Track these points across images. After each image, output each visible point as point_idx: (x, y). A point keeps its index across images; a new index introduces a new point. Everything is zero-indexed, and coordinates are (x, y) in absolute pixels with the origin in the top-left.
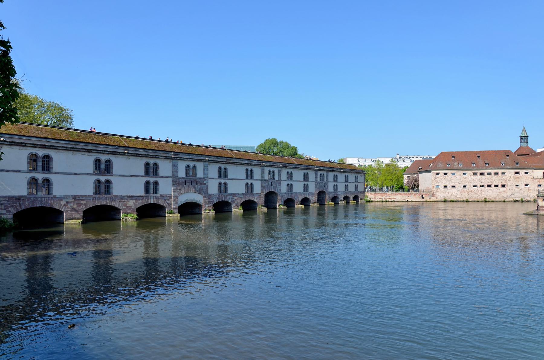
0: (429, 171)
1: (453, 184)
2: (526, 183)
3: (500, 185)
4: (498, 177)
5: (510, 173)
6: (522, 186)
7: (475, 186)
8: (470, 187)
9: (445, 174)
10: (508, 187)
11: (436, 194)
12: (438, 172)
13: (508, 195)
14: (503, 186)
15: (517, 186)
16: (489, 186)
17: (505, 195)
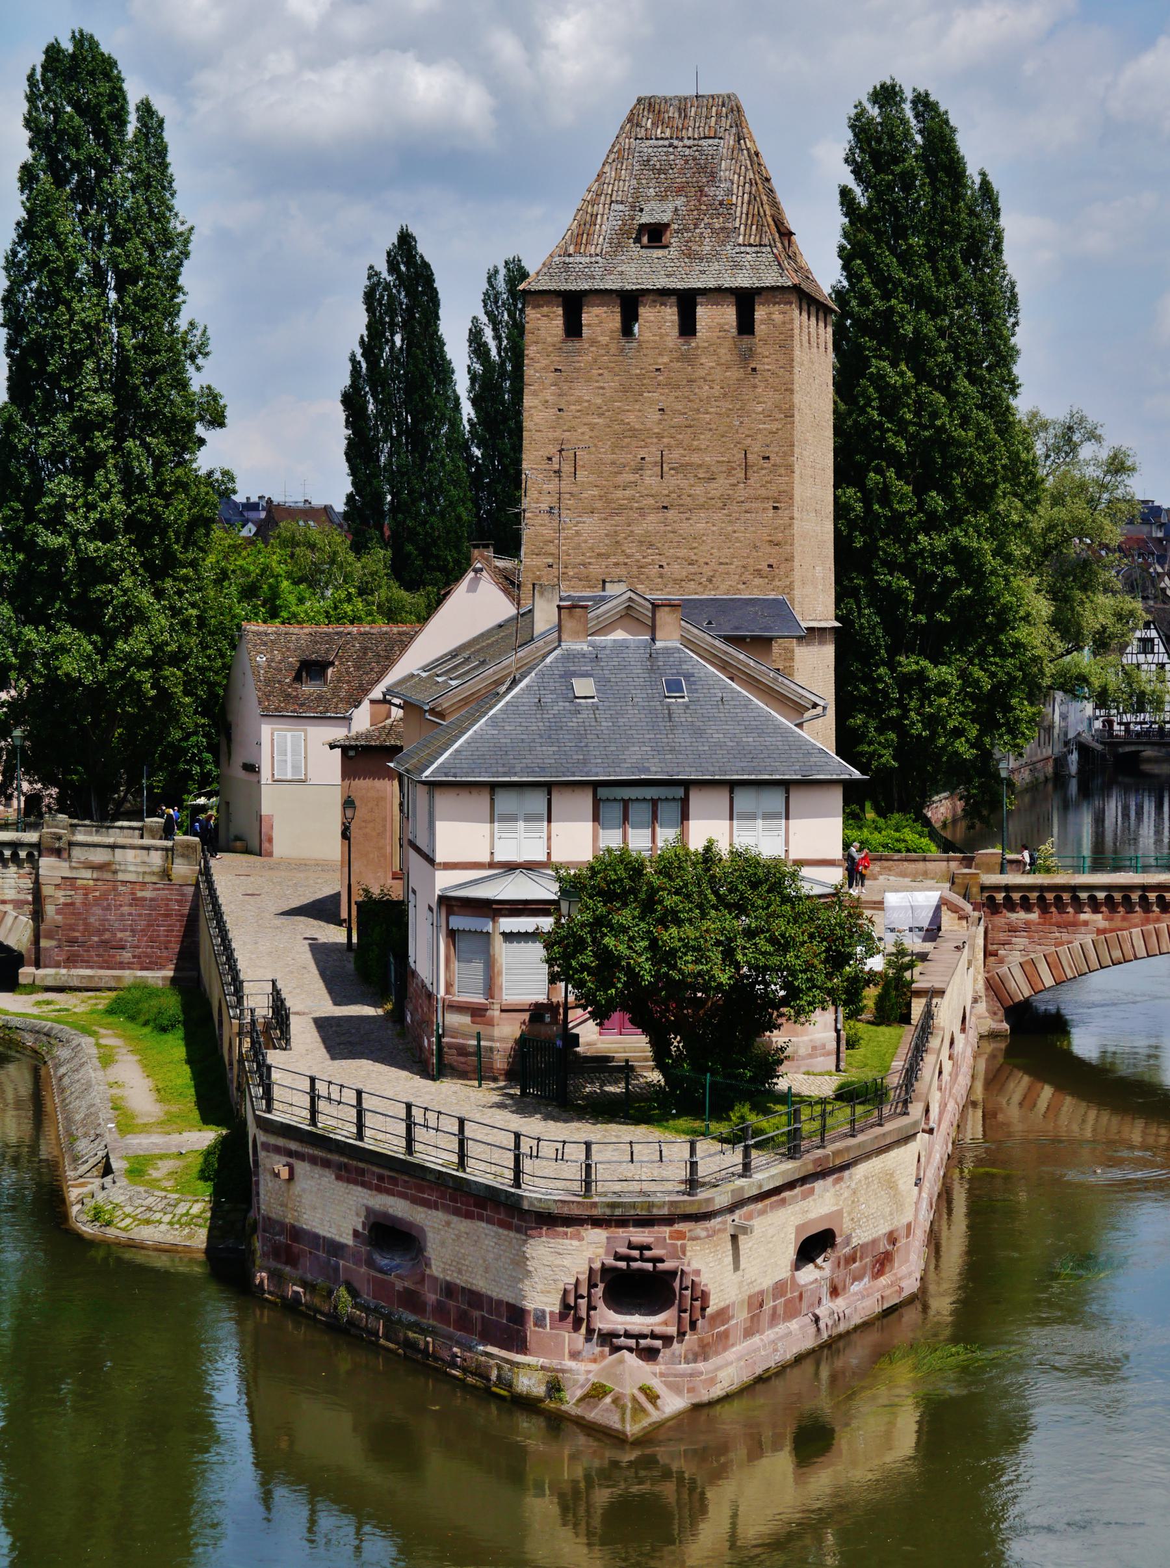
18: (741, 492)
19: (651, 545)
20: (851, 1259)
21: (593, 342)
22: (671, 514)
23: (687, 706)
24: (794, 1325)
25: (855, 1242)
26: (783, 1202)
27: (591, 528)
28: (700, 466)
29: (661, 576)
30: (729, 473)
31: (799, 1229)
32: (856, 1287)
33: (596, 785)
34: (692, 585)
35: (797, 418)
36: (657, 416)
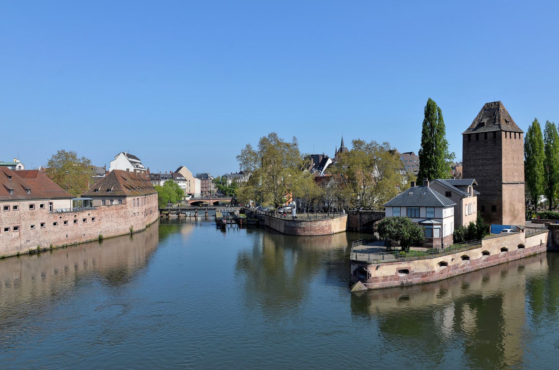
2: (42, 222)
3: (12, 228)
4: (9, 214)
5: (24, 205)
10: (22, 230)
13: (23, 243)
14: (16, 228)
15: (32, 227)
17: (17, 244)
18: (494, 162)
19: (481, 171)
20: (413, 275)
21: (472, 141)
22: (484, 166)
23: (424, 196)
24: (396, 282)
25: (415, 272)
26: (392, 264)
27: (472, 169)
28: (488, 159)
29: (482, 176)
30: (492, 160)
31: (397, 268)
32: (416, 278)
33: (407, 207)
34: (487, 177)
35: (503, 150)
36: (481, 152)
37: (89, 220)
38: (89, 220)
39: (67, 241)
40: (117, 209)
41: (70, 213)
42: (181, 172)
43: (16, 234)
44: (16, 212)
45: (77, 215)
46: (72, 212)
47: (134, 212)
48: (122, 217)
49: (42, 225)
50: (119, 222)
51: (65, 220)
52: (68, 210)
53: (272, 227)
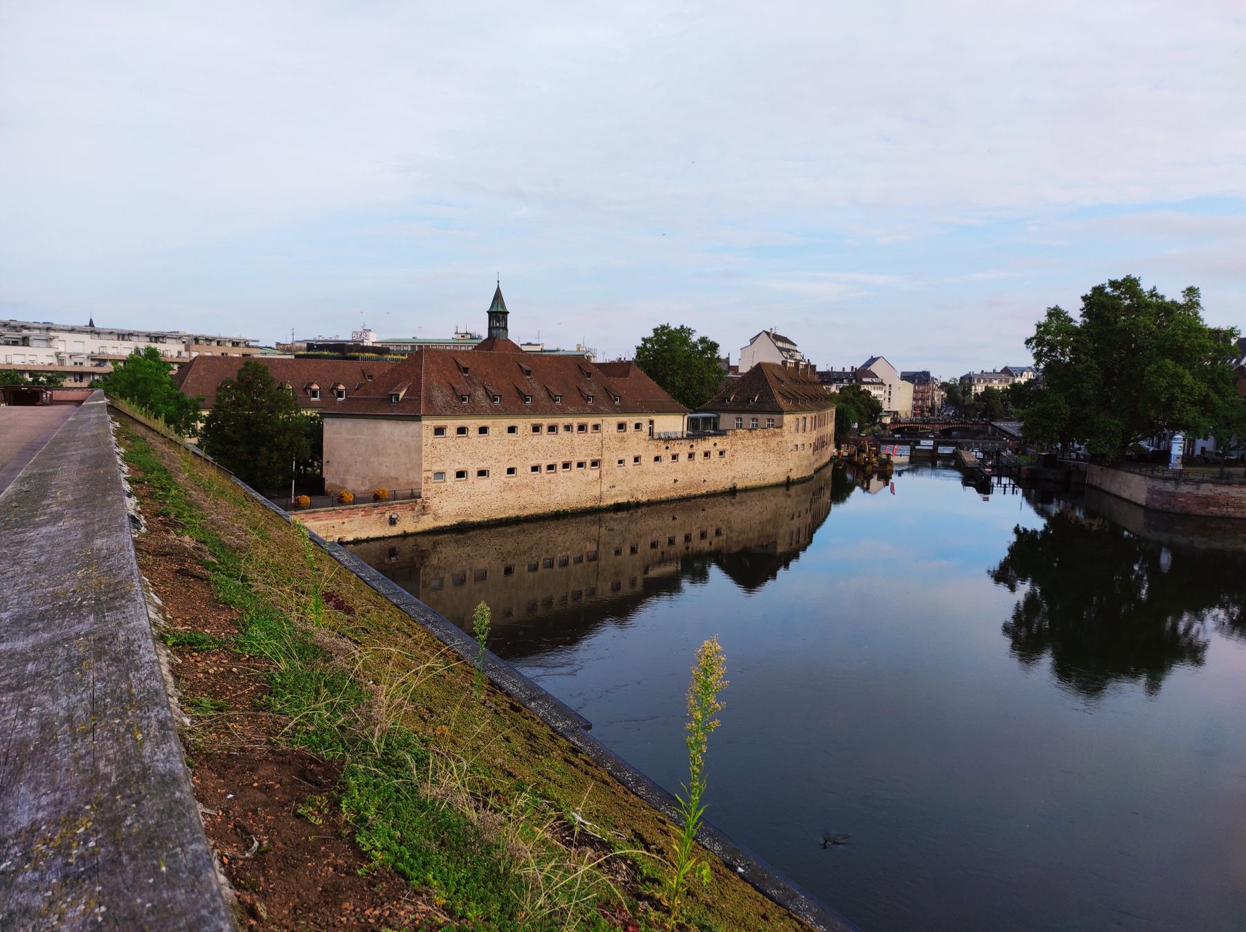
0: (417, 418)
1: (483, 466)
2: (637, 454)
3: (588, 464)
5: (609, 423)
6: (630, 462)
7: (535, 469)
8: (523, 470)
9: (462, 431)
10: (605, 467)
11: (434, 503)
12: (440, 423)
13: (605, 488)
14: (594, 464)
15: (620, 462)
16: (566, 465)
37: (715, 455)
38: (715, 455)
39: (675, 489)
40: (764, 436)
41: (683, 441)
42: (873, 368)
43: (594, 473)
44: (596, 435)
45: (694, 444)
46: (686, 439)
47: (795, 443)
48: (772, 451)
49: (636, 459)
50: (768, 460)
51: (673, 452)
52: (680, 436)
53: (1107, 489)
